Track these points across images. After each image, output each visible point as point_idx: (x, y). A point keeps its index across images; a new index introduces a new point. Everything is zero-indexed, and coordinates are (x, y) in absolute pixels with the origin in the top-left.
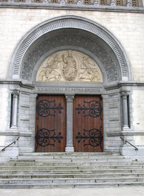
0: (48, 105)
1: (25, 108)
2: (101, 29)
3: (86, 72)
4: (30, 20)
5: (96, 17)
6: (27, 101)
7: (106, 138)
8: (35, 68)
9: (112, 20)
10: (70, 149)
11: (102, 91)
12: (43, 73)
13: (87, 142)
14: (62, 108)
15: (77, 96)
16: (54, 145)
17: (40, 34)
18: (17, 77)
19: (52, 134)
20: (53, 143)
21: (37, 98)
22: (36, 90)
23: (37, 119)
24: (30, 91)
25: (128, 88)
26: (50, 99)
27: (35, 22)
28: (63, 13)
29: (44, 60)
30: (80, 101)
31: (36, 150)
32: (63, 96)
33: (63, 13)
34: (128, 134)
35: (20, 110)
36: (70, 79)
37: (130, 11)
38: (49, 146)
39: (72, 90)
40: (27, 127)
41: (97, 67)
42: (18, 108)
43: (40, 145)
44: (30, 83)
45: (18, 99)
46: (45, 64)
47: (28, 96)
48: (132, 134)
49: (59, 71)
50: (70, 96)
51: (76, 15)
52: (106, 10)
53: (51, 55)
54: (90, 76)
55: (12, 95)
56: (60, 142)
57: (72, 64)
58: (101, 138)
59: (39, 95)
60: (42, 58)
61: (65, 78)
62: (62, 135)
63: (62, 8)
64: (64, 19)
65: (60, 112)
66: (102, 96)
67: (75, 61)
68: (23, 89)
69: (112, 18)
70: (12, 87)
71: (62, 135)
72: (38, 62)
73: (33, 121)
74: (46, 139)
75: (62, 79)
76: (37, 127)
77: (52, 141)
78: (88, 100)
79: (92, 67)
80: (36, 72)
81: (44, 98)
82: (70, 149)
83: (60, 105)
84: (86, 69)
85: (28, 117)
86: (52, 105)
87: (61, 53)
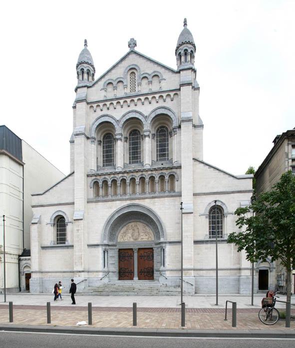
0: (124, 255)
2: (149, 210)
3: (144, 235)
4: (111, 208)
5: (147, 203)
6: (113, 254)
7: (155, 272)
8: (117, 235)
9: (157, 204)
10: (136, 278)
11: (154, 246)
12: (121, 237)
13: (145, 274)
14: (132, 256)
15: (139, 249)
17: (116, 216)
18: (106, 242)
21: (119, 251)
22: (118, 247)
23: (119, 262)
24: (114, 248)
25: (164, 245)
26: (126, 251)
27: (114, 209)
29: (121, 229)
30: (142, 252)
31: (119, 279)
32: (132, 249)
33: (128, 202)
34: (162, 271)
35: (109, 259)
36: (136, 239)
37: (167, 196)
40: (113, 266)
41: (151, 231)
42: (107, 258)
44: (115, 243)
46: (122, 231)
48: (165, 271)
49: (130, 235)
50: (135, 249)
52: (153, 198)
53: (125, 225)
54: (147, 237)
57: (137, 231)
58: (153, 272)
59: (120, 250)
60: (121, 228)
61: (133, 239)
62: (132, 271)
64: (129, 206)
66: (154, 249)
67: (138, 229)
68: (111, 247)
70: (104, 247)
71: (132, 271)
72: (118, 231)
73: (117, 264)
74: (124, 273)
75: (132, 240)
76: (119, 267)
78: (147, 251)
79: (148, 231)
82: (136, 278)
83: (131, 254)
85: (114, 262)
87: (130, 224)
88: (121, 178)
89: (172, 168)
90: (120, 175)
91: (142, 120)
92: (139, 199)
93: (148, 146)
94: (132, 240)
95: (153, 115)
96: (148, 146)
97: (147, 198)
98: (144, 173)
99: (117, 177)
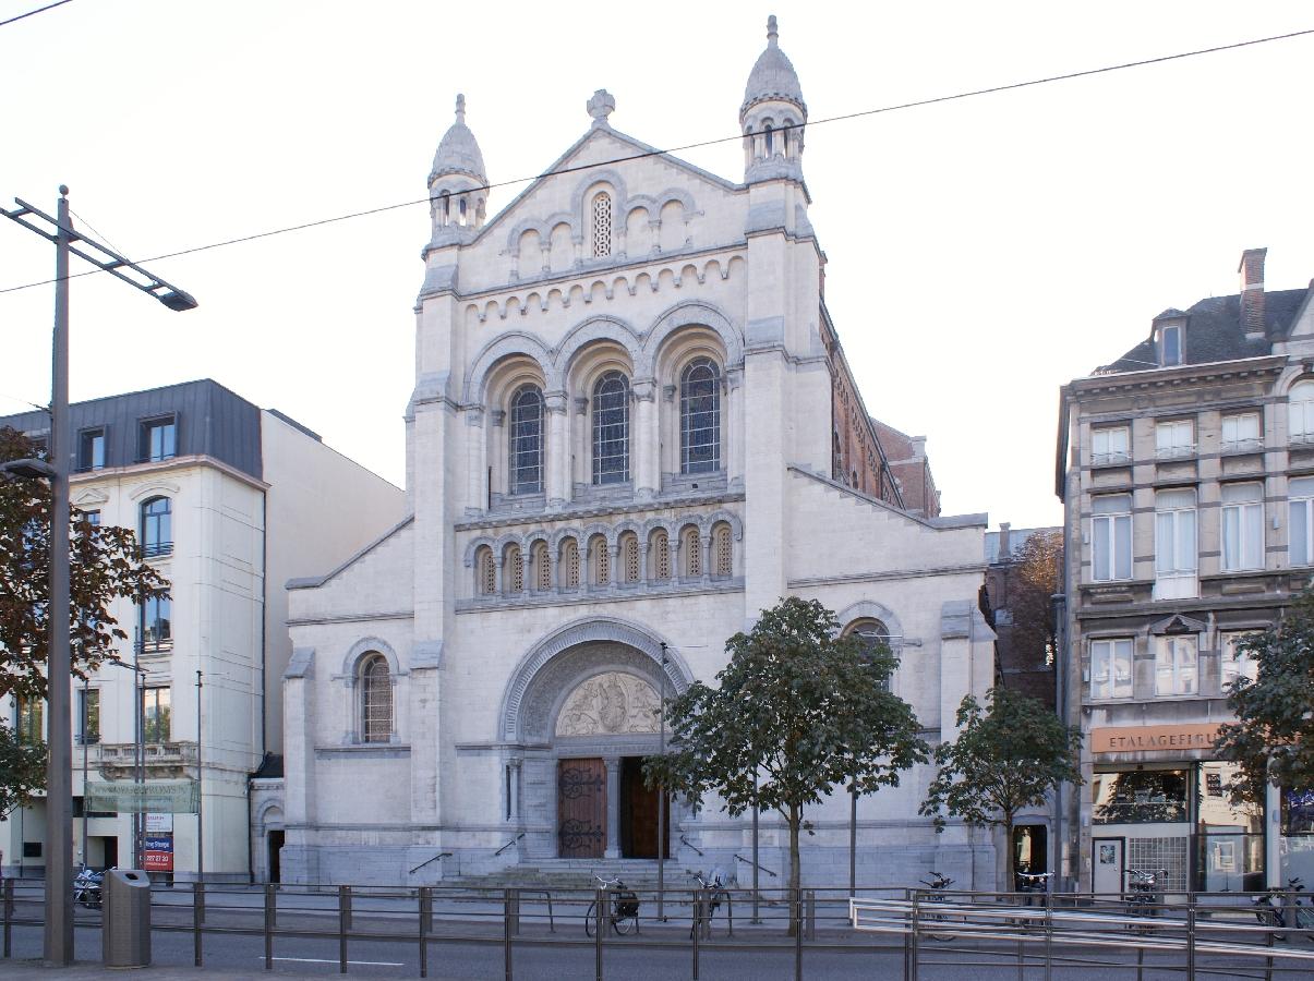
1: (536, 786)
4: (529, 631)
6: (541, 773)
8: (552, 713)
9: (671, 616)
16: (589, 846)
19: (586, 829)
20: (587, 843)
22: (557, 752)
24: (544, 754)
27: (539, 635)
28: (583, 612)
29: (568, 695)
31: (561, 855)
33: (583, 612)
36: (613, 728)
37: (706, 593)
38: (582, 848)
39: (616, 749)
43: (568, 846)
44: (545, 741)
45: (519, 773)
46: (570, 703)
47: (542, 764)
49: (595, 715)
50: (612, 761)
51: (605, 613)
55: (508, 767)
56: (599, 841)
59: (562, 762)
61: (605, 726)
63: (581, 602)
64: (583, 626)
65: (599, 790)
68: (528, 754)
69: (668, 613)
73: (552, 807)
75: (601, 730)
77: (586, 840)
80: (556, 719)
81: (572, 765)
84: (644, 707)
85: (543, 801)
86: (585, 777)
88: (562, 535)
89: (720, 501)
90: (559, 525)
91: (630, 347)
92: (615, 601)
93: (652, 428)
94: (601, 730)
95: (664, 329)
96: (652, 428)
97: (639, 598)
98: (633, 516)
99: (549, 531)
